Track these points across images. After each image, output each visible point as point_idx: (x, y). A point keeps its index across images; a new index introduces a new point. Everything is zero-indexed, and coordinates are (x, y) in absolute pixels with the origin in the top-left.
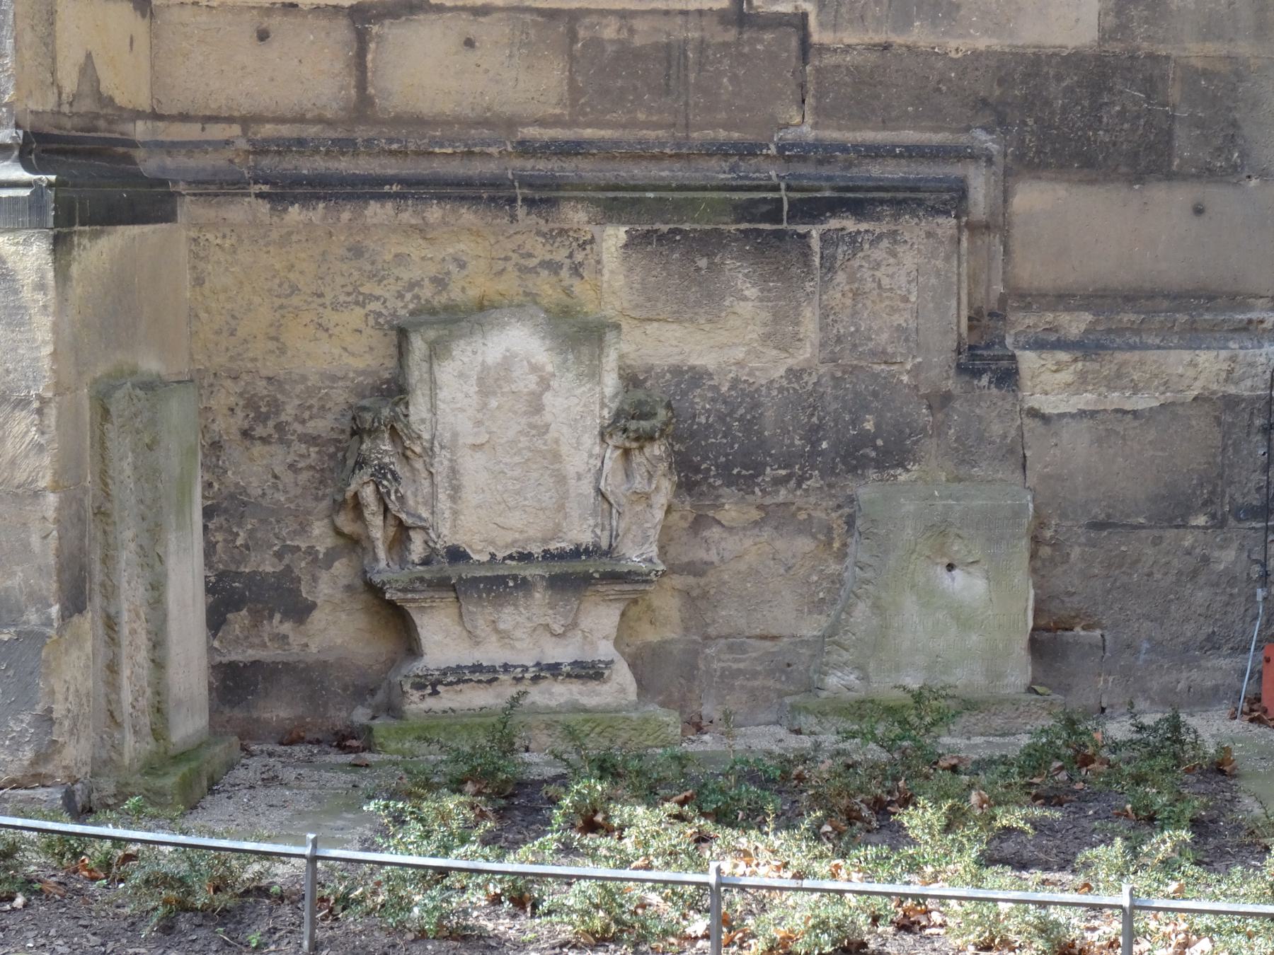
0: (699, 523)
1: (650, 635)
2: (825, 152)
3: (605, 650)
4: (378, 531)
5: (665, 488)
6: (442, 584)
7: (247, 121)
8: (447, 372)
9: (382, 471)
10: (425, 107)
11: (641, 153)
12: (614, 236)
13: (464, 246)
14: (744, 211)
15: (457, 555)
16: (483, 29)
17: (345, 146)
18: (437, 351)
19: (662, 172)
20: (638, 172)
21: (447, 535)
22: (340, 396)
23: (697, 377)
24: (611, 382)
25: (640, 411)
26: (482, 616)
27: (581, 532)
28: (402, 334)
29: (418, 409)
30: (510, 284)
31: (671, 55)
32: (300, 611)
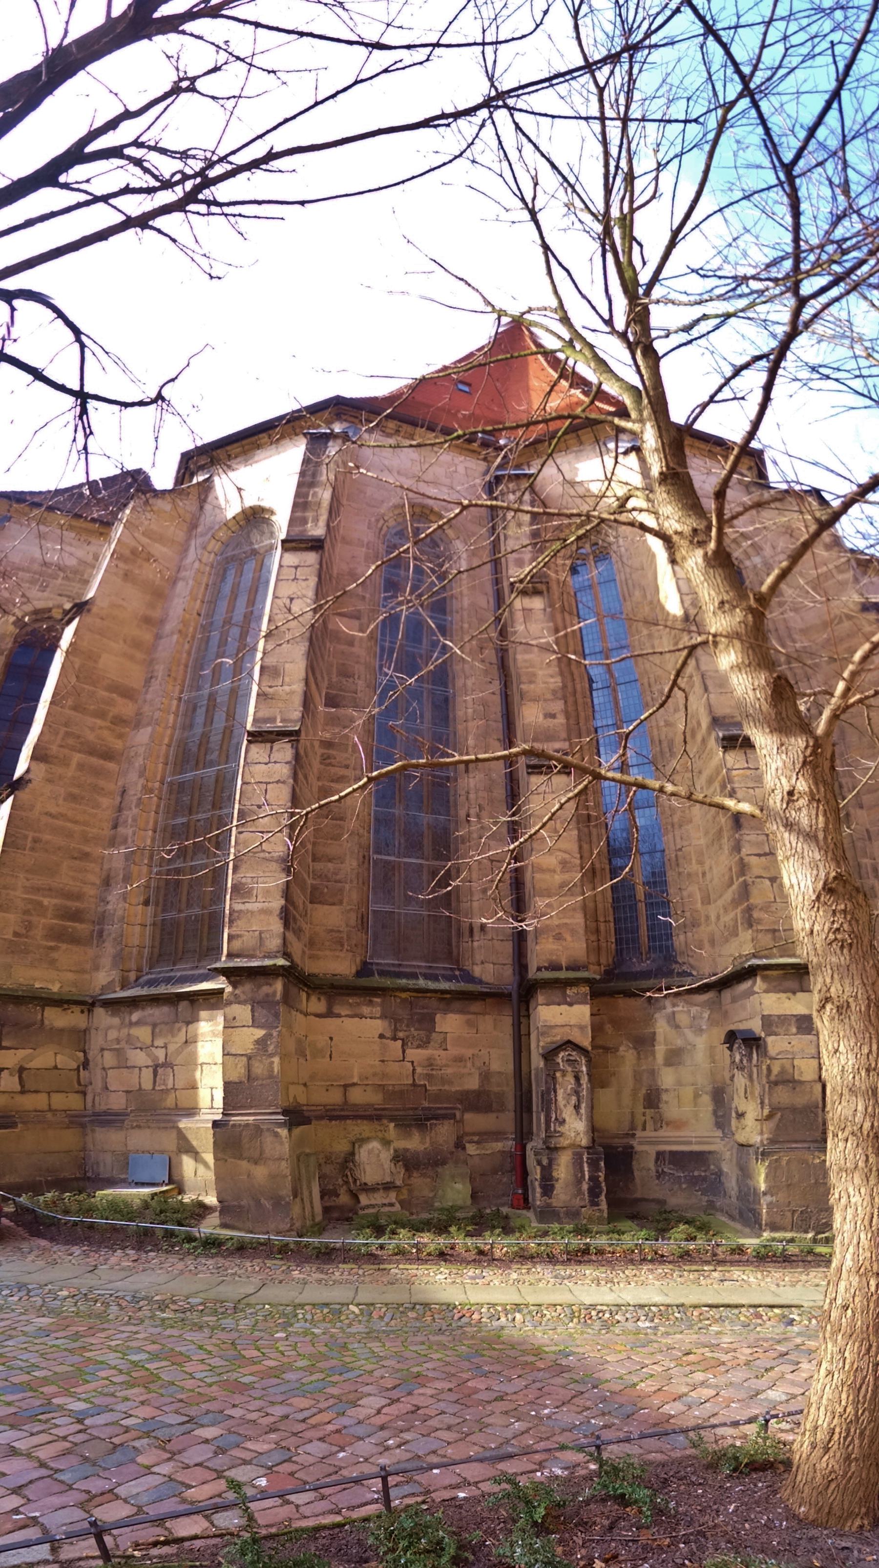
0: (409, 1177)
1: (402, 1197)
2: (429, 1109)
3: (394, 1200)
4: (351, 1180)
5: (403, 1171)
6: (363, 1190)
7: (324, 1106)
8: (362, 1150)
9: (351, 1169)
10: (357, 1102)
11: (397, 1110)
12: (392, 1125)
13: (365, 1127)
14: (415, 1120)
15: (365, 1184)
16: (368, 1088)
17: (342, 1110)
18: (360, 1146)
19: (401, 1113)
20: (396, 1113)
21: (363, 1180)
22: (342, 1155)
23: (407, 1150)
24: (392, 1151)
25: (398, 1156)
26: (371, 1195)
27: (388, 1179)
28: (354, 1144)
29: (357, 1157)
30: (373, 1134)
31: (402, 1092)
32: (338, 1196)
